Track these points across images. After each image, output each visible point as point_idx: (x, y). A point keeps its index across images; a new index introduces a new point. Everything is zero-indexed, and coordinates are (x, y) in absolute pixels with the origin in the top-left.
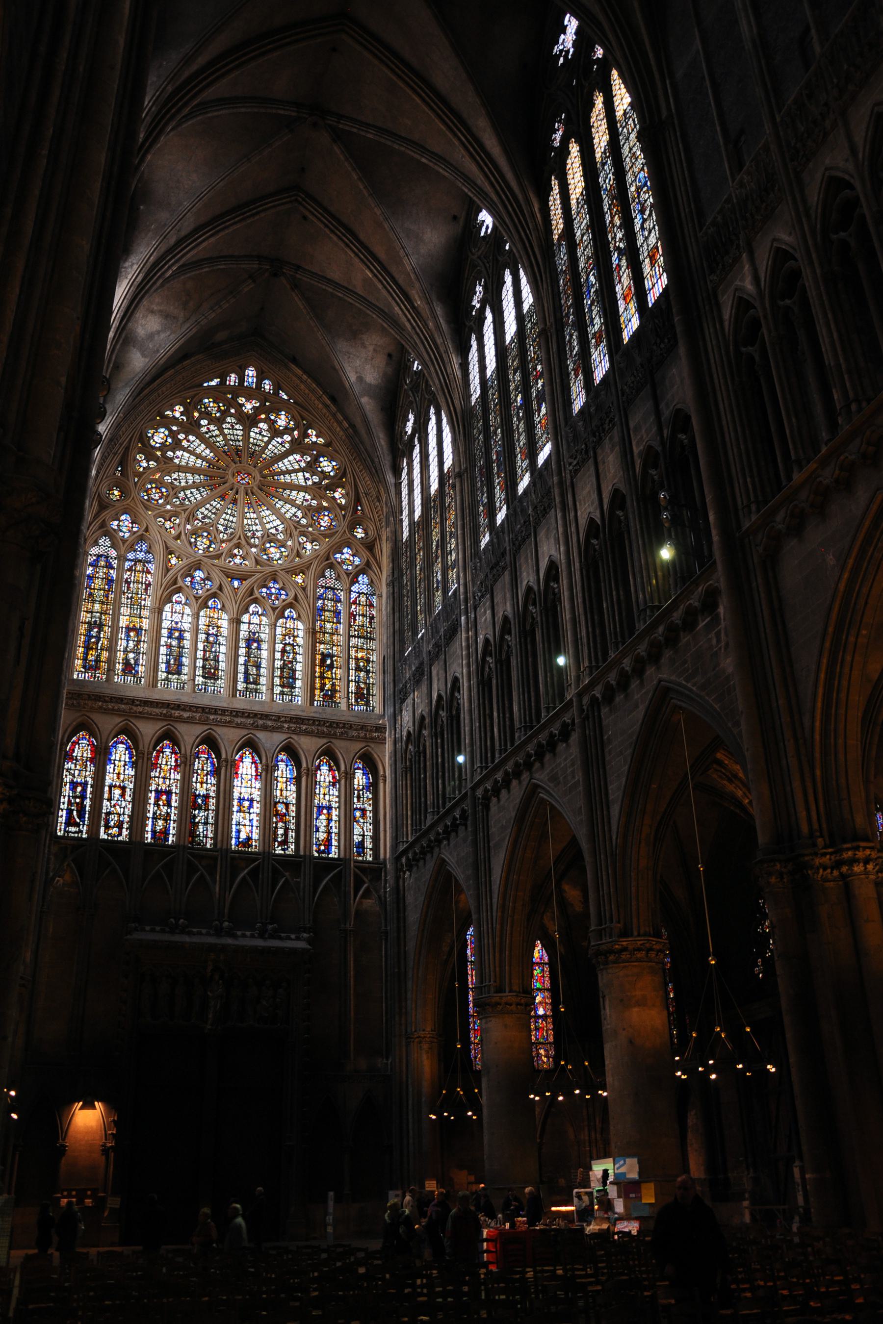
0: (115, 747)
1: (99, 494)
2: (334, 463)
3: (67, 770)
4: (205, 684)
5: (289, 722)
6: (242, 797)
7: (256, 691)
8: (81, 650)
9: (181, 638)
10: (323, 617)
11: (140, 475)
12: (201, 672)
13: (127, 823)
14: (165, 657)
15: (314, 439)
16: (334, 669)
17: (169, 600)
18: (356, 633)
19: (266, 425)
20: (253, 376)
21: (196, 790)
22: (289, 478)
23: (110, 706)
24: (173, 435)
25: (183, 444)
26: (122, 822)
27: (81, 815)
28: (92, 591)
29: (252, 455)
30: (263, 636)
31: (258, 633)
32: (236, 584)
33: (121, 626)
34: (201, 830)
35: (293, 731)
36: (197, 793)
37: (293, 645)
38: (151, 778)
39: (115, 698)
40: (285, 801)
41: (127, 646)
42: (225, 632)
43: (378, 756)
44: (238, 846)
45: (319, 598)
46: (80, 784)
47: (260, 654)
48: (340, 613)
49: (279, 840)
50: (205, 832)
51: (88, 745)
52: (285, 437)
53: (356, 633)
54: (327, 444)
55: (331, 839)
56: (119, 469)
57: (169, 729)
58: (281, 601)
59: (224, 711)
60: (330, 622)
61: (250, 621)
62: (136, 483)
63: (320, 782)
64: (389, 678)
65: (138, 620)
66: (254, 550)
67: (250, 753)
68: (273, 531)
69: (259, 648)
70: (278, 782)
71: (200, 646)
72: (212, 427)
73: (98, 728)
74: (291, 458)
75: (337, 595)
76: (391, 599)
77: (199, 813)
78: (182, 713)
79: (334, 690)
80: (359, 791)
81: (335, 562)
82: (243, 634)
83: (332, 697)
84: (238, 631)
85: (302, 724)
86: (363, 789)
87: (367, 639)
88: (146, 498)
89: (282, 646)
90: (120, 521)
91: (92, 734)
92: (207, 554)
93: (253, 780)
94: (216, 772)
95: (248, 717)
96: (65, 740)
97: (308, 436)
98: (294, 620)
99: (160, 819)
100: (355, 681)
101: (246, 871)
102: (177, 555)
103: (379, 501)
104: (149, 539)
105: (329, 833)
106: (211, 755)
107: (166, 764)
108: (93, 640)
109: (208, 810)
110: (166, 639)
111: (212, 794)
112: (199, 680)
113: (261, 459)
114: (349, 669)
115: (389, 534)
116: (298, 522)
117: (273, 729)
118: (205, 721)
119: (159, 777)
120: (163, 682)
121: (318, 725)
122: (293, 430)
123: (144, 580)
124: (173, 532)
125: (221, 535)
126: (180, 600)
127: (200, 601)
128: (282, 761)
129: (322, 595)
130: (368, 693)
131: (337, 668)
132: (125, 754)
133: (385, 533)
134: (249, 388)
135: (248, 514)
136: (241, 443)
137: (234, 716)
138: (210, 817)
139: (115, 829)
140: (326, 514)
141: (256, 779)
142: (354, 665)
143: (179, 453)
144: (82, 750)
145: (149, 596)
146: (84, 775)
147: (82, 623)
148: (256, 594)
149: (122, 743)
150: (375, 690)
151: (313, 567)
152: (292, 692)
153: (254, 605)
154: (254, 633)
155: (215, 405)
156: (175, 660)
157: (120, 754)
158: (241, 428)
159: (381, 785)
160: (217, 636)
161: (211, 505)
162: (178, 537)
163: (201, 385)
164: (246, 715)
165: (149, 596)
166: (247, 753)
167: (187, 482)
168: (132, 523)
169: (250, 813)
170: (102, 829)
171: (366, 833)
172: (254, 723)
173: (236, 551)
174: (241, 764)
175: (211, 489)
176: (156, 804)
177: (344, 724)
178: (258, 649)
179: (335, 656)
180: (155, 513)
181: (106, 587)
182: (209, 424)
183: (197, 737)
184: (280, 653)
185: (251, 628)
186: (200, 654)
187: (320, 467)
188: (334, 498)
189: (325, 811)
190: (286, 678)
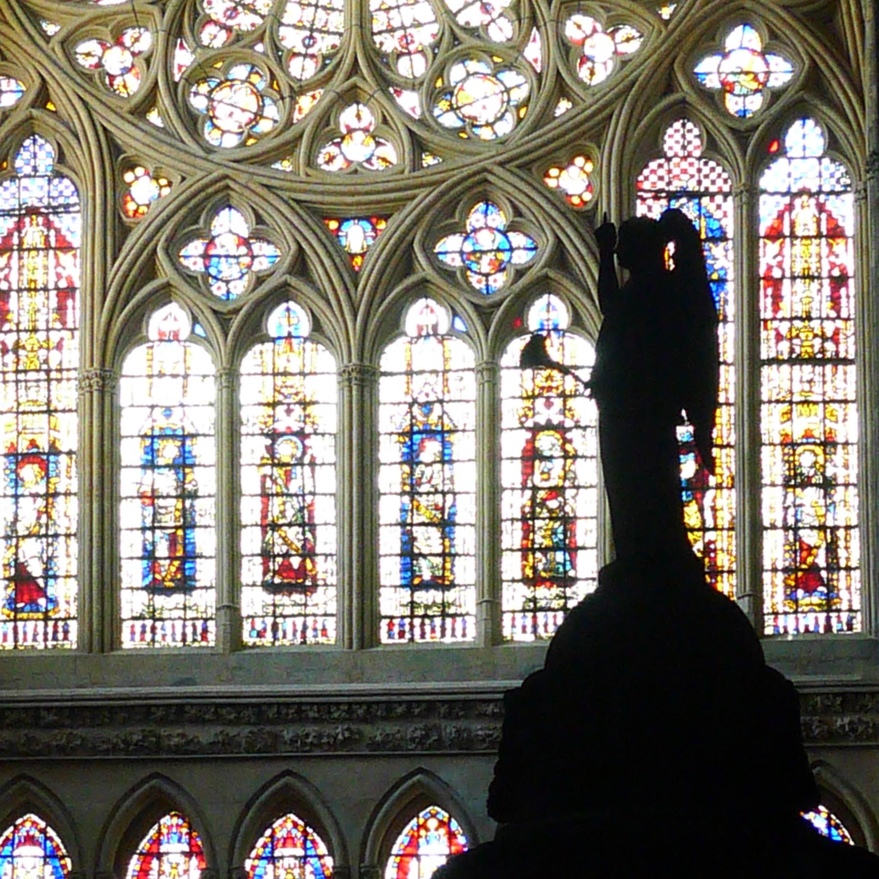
18: (784, 346)
31: (441, 402)
37: (561, 429)
43: (857, 794)
47: (451, 479)
53: (784, 346)
67: (442, 824)
78: (192, 732)
81: (692, 98)
87: (823, 362)
95: (407, 716)
100: (786, 528)
120: (138, 624)
137: (364, 720)
151: (615, 130)
153: (422, 302)
156: (173, 541)
164: (400, 710)
165: (72, 330)
172: (427, 736)
178: (443, 462)
183: (248, 807)
190: (545, 550)
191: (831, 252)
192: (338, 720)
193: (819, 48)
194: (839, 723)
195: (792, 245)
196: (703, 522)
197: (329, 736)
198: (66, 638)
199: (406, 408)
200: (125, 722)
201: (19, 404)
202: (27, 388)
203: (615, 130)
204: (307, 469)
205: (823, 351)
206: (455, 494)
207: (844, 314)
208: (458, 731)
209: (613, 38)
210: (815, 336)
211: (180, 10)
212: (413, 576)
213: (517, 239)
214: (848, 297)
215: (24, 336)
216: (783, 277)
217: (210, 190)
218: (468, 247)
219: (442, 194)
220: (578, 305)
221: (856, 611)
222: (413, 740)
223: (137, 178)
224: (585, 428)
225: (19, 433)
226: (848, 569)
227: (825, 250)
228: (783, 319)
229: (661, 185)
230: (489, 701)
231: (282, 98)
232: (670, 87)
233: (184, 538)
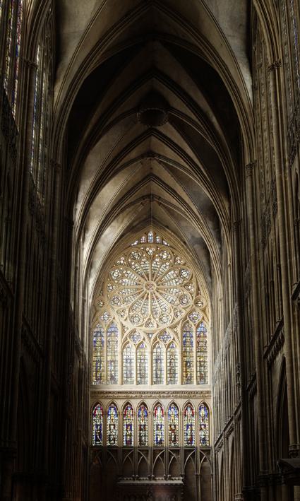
9: (130, 363)
17: (124, 348)
27: (100, 437)
54: (184, 264)
59: (148, 392)
69: (161, 363)
74: (169, 273)
79: (191, 377)
82: (154, 357)
83: (190, 379)
105: (192, 436)
112: (139, 379)
117: (169, 397)
143: (124, 280)
144: (99, 412)
151: (180, 325)
157: (112, 412)
163: (130, 246)
176: (126, 430)
203: (180, 325)
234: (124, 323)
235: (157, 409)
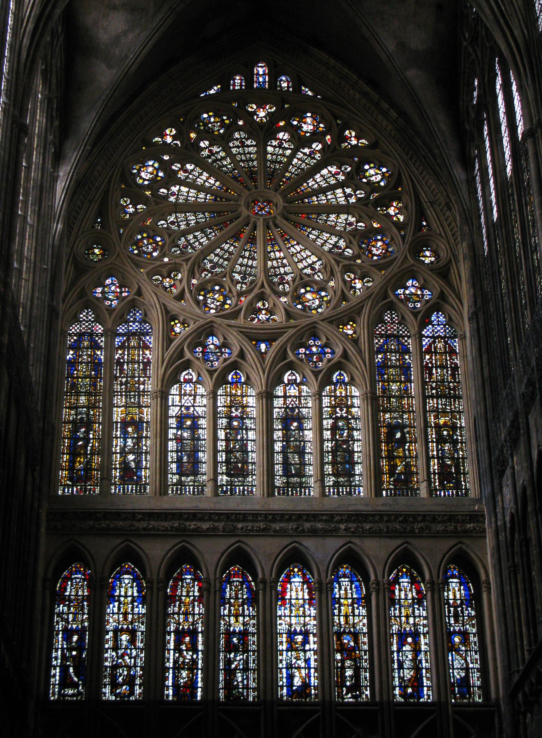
0: (120, 580)
1: (74, 257)
2: (384, 170)
3: (60, 615)
4: (230, 483)
5: (348, 521)
6: (293, 629)
7: (301, 485)
8: (66, 457)
9: (195, 427)
10: (386, 376)
11: (125, 224)
12: (224, 468)
13: (140, 677)
14: (175, 455)
15: (354, 142)
16: (408, 444)
17: (174, 379)
18: (434, 391)
19: (287, 134)
20: (264, 74)
21: (230, 625)
22: (323, 198)
23: (103, 525)
24: (165, 166)
25: (179, 176)
26: (134, 677)
28: (75, 381)
29: (271, 175)
30: (304, 411)
31: (299, 408)
32: (263, 347)
33: (115, 420)
34: (240, 679)
35: (353, 532)
36: (232, 629)
37: (346, 419)
38: (168, 615)
39: (109, 513)
40: (352, 630)
41: (125, 444)
42: (253, 412)
43: (477, 556)
44: (291, 697)
45: (379, 352)
46: (76, 632)
48: (409, 367)
49: (348, 684)
50: (245, 681)
51: (84, 581)
52: (314, 146)
54: (373, 146)
55: (422, 677)
56: (99, 220)
57: (183, 545)
58: (325, 360)
59: (255, 516)
60: (397, 382)
61: (285, 393)
62: (120, 235)
63: (400, 599)
64: (483, 445)
65: (137, 410)
66: (283, 299)
68: (308, 271)
69: (301, 428)
70: (341, 605)
71: (221, 434)
72: (215, 149)
73: (91, 555)
74: (324, 172)
75: (403, 344)
76: (476, 338)
77: (235, 656)
78: (199, 524)
79: (408, 473)
80: (456, 608)
81: (395, 300)
84: (270, 408)
85: (365, 522)
86: (462, 603)
87: (450, 398)
88: (136, 252)
89: (331, 421)
90: (104, 286)
91: (87, 566)
92: (221, 313)
93: (307, 606)
94: (252, 600)
95: (289, 520)
96: (50, 575)
97: (346, 139)
98: (346, 384)
99: (183, 669)
100: (438, 458)
101: (300, 730)
102: (181, 320)
103: (450, 209)
104: (144, 304)
105: (417, 668)
106: (247, 577)
107: (188, 596)
108: (80, 443)
109: (247, 651)
110: (175, 431)
111: (251, 629)
112: (223, 479)
113: (284, 180)
114: (427, 443)
115: (466, 250)
116: (341, 255)
117: (326, 533)
118: (230, 531)
119: (178, 614)
120: (175, 487)
121: (387, 521)
122: (324, 134)
123: (141, 358)
124: (174, 290)
125: (239, 286)
126: (191, 377)
127: (216, 375)
128: (345, 576)
129: (382, 346)
130: (458, 472)
131: (411, 442)
132: (132, 587)
133: (463, 249)
134: (262, 89)
135: (272, 254)
136: (255, 163)
137: (271, 521)
138: (251, 659)
139: (124, 687)
140: (379, 237)
141: (310, 605)
142: (434, 436)
143: (175, 189)
145: (149, 377)
146: (80, 619)
147: (65, 422)
148: (291, 357)
149: (128, 573)
150: (468, 467)
151: (366, 310)
152: (351, 482)
153: (290, 372)
154: (293, 409)
155: (217, 120)
158: (254, 143)
159: (485, 596)
160: (242, 418)
161: (222, 249)
162: (180, 297)
164: (286, 517)
165: (149, 377)
166: (296, 570)
167: (188, 224)
168: (120, 287)
169: (305, 651)
170: (107, 690)
171: (471, 666)
172: (298, 528)
173: (260, 304)
174: (289, 586)
175: (221, 229)
176: (177, 649)
177: (424, 516)
179: (405, 426)
180: (148, 270)
181: (93, 373)
182: (210, 145)
183: (223, 554)
184: (329, 433)
185: (288, 402)
186: (221, 445)
187: (366, 177)
188: (388, 216)
189: (410, 640)
190: (340, 463)
191: (451, 358)
192: (261, 521)
193: (443, 284)
194: (468, 526)
195: (436, 356)
196: (405, 454)
197: (257, 527)
198: (145, 491)
199: (283, 410)
200: (171, 520)
201: (127, 404)
202: (130, 398)
204: (244, 432)
205: (449, 393)
206: (305, 442)
207: (457, 380)
208: (311, 526)
209: (363, 281)
210: (446, 388)
211: (193, 264)
212: (287, 473)
213: (328, 350)
214: (458, 374)
215: (129, 379)
216: (432, 367)
217: (206, 327)
218: (307, 352)
219: (298, 330)
220: (353, 373)
221: (469, 489)
222: (292, 529)
223: (176, 324)
224: (356, 419)
225: (127, 415)
226: (464, 474)
227: (448, 358)
228: (433, 382)
229: (383, 332)
230: (324, 515)
231: (234, 296)
232: (386, 296)
233: (194, 455)
234: (174, 306)
235: (288, 580)
